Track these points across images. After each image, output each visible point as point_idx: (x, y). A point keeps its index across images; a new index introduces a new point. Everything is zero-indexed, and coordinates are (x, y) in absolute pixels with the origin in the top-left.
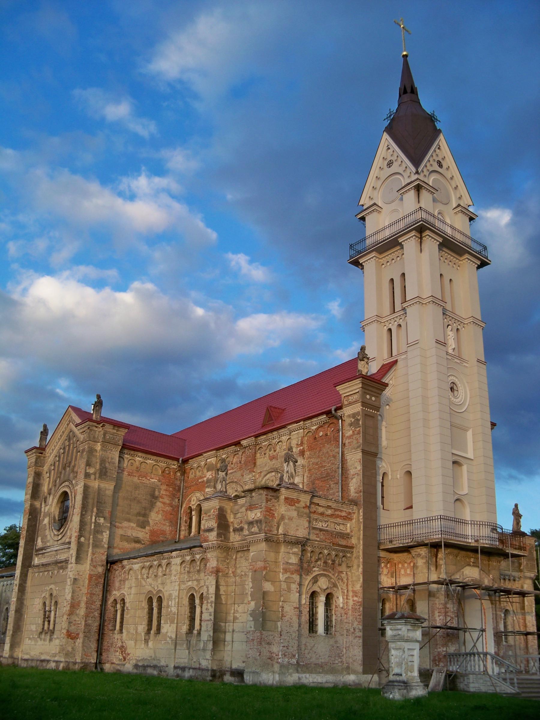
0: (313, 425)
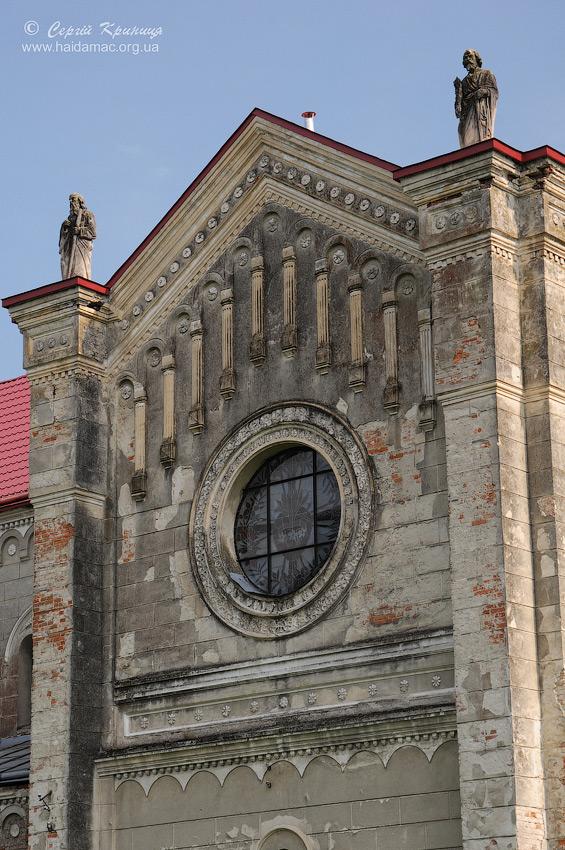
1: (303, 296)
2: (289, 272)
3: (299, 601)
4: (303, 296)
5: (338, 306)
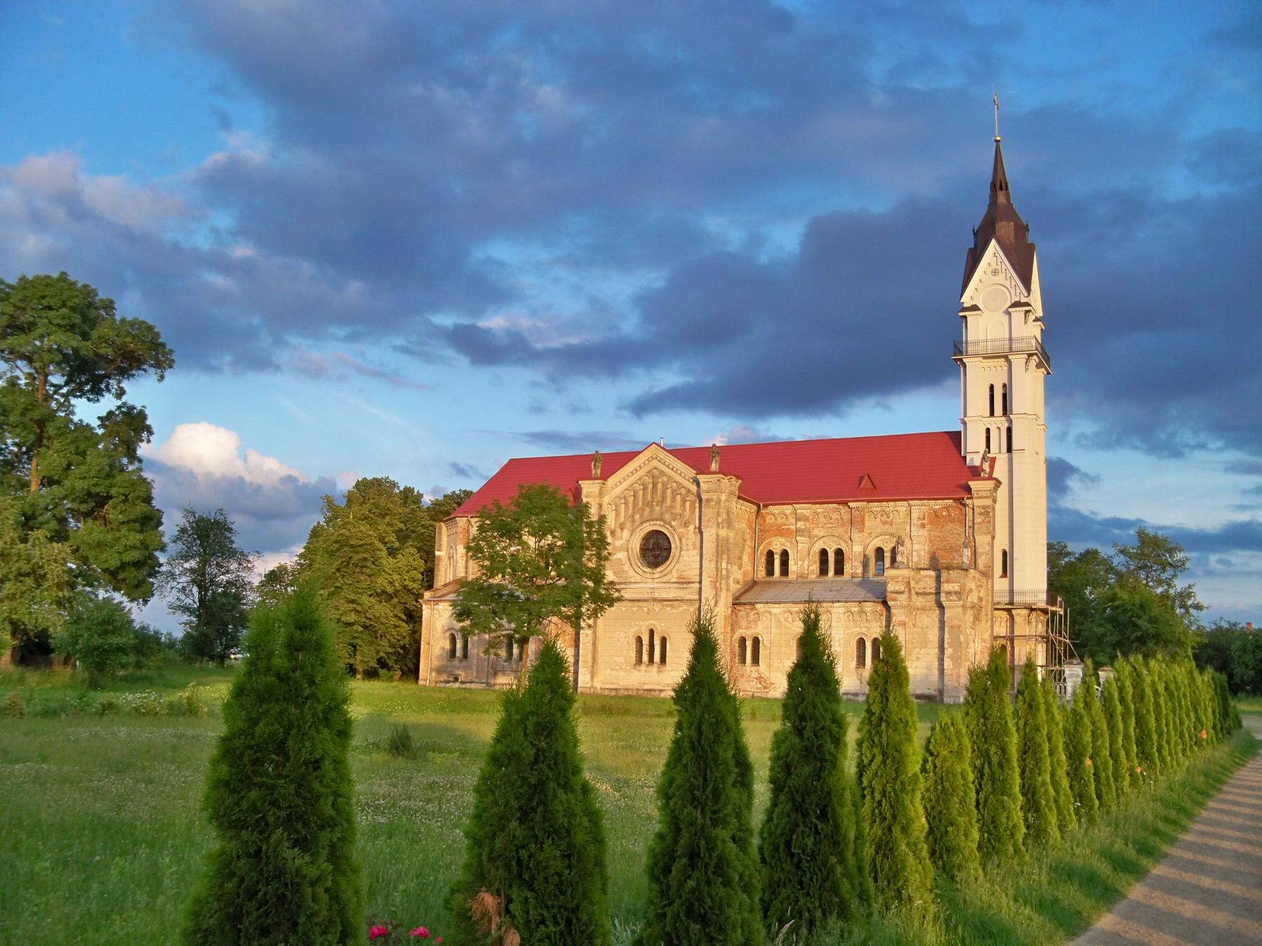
0: (938, 505)
1: (664, 493)
2: (660, 486)
3: (659, 569)
4: (664, 493)
5: (673, 500)
